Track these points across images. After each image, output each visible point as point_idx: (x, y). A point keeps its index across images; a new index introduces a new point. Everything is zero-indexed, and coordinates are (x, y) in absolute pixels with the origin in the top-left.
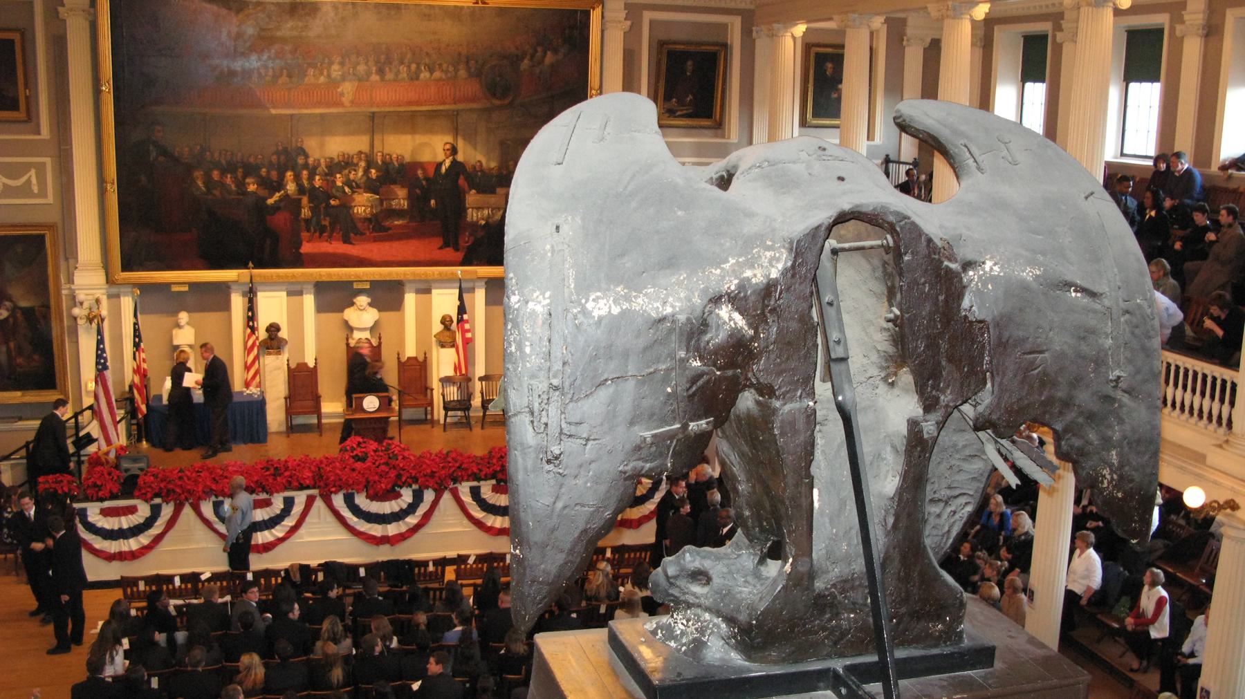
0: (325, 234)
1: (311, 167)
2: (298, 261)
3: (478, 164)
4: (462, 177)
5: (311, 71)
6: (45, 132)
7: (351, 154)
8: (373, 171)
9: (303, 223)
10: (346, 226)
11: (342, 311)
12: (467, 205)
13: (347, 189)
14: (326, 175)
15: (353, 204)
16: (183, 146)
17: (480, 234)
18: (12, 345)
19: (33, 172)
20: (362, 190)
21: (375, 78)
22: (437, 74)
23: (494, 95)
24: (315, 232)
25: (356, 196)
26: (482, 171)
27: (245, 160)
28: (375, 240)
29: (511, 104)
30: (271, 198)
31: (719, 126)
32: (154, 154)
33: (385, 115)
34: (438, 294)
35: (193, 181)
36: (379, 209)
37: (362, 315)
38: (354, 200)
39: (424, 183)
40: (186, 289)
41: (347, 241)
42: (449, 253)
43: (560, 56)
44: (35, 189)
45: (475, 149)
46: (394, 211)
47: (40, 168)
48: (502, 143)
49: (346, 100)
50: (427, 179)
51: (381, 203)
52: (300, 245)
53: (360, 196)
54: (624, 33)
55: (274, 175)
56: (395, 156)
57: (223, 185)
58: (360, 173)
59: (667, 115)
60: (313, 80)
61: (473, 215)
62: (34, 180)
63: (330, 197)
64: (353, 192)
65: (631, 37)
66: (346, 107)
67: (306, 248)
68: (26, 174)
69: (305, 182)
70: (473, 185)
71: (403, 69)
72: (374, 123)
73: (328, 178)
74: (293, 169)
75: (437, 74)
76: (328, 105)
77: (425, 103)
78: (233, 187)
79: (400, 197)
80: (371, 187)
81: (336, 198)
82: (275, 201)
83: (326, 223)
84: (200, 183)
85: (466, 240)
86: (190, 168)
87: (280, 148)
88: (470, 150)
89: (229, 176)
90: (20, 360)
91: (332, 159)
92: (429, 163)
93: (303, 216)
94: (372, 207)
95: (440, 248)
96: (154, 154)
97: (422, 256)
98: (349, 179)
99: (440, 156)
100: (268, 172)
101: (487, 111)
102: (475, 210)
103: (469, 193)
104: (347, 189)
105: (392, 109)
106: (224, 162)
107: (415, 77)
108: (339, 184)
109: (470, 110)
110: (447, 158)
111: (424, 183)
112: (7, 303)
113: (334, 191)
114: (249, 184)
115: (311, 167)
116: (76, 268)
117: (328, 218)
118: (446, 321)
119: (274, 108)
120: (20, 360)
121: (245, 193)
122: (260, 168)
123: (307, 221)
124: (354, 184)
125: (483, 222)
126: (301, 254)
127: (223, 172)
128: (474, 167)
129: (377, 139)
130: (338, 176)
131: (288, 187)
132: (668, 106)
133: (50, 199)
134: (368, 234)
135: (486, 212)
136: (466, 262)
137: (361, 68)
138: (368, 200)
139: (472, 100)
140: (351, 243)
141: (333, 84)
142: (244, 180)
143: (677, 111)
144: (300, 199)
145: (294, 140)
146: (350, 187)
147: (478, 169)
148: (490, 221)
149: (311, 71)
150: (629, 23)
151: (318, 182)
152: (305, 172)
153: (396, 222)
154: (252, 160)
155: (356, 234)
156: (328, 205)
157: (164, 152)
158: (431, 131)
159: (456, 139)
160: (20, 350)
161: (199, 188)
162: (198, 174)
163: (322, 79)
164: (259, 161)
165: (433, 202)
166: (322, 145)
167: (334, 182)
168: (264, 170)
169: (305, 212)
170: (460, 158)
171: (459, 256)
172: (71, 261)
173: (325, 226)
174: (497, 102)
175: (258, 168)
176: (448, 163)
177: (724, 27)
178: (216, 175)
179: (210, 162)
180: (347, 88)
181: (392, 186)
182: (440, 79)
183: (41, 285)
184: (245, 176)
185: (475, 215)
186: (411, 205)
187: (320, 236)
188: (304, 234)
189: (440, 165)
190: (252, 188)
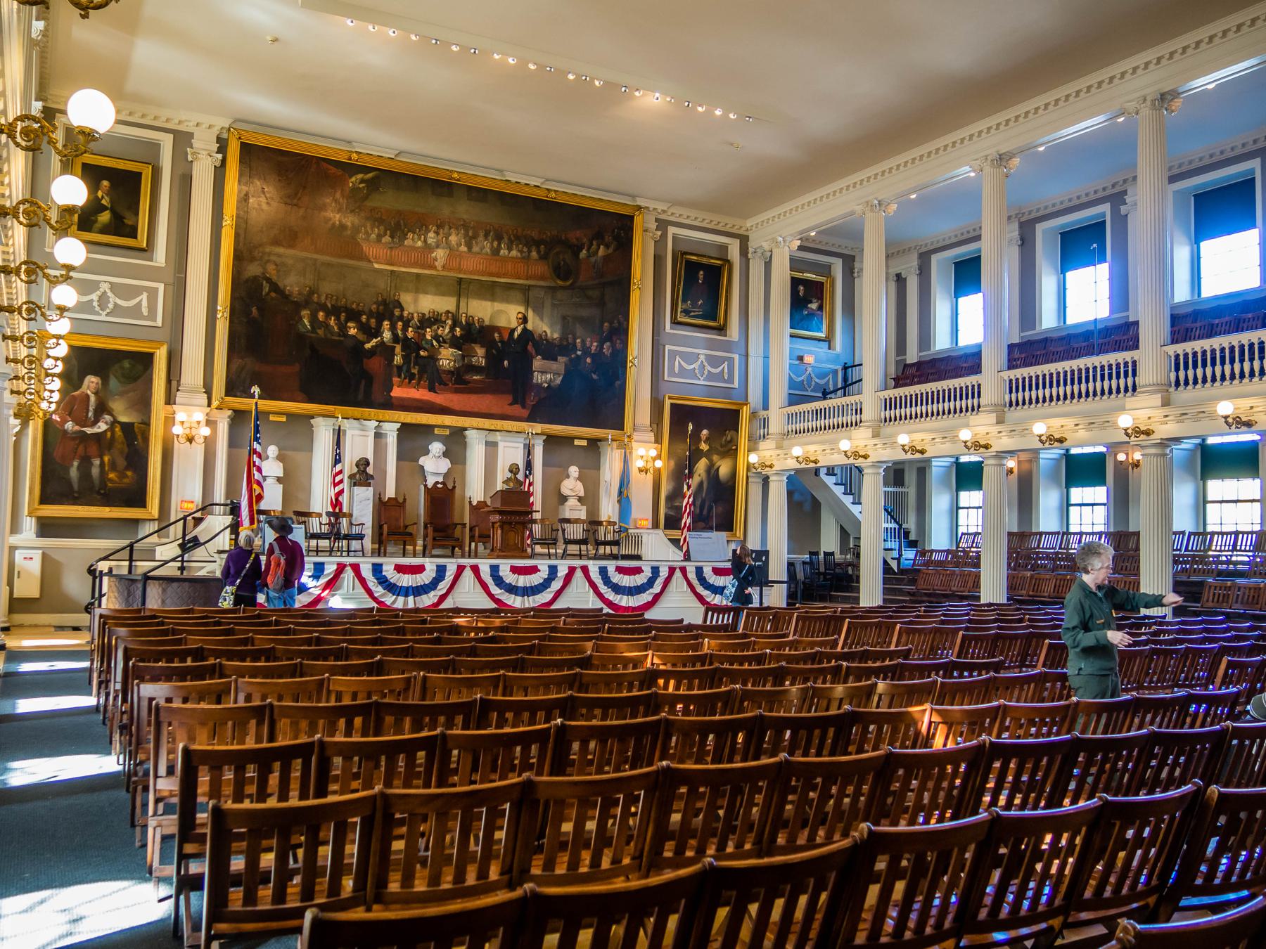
2: (390, 405)
5: (410, 235)
6: (160, 255)
8: (458, 329)
9: (395, 369)
10: (433, 377)
13: (435, 343)
14: (418, 328)
17: (543, 395)
18: (106, 459)
19: (144, 296)
21: (464, 248)
22: (514, 253)
23: (559, 277)
25: (442, 350)
27: (349, 306)
28: (457, 391)
29: (571, 287)
31: (722, 330)
33: (470, 281)
35: (301, 318)
42: (517, 409)
43: (610, 251)
44: (145, 313)
45: (542, 319)
46: (474, 366)
47: (153, 293)
48: (564, 318)
49: (439, 264)
50: (501, 341)
51: (463, 360)
55: (373, 321)
57: (327, 326)
58: (447, 330)
61: (538, 378)
62: (145, 303)
63: (421, 348)
64: (440, 346)
65: (660, 243)
67: (397, 392)
69: (400, 333)
71: (487, 245)
72: (461, 288)
74: (390, 320)
75: (514, 253)
76: (423, 267)
77: (505, 276)
79: (479, 355)
80: (455, 343)
81: (425, 349)
83: (415, 371)
84: (306, 321)
86: (298, 306)
87: (380, 299)
90: (112, 475)
91: (424, 314)
92: (505, 328)
94: (455, 361)
95: (511, 404)
96: (267, 289)
99: (514, 324)
100: (368, 319)
101: (553, 290)
104: (435, 343)
105: (476, 277)
106: (329, 305)
107: (496, 252)
108: (428, 337)
109: (540, 287)
112: (108, 418)
116: (178, 390)
118: (514, 469)
119: (377, 263)
120: (112, 475)
121: (346, 335)
123: (399, 368)
127: (328, 315)
128: (540, 335)
133: (159, 322)
135: (549, 376)
136: (531, 419)
137: (453, 239)
139: (542, 278)
141: (428, 248)
142: (346, 323)
145: (392, 293)
146: (438, 341)
149: (410, 235)
150: (659, 233)
151: (410, 334)
152: (400, 323)
154: (354, 306)
157: (275, 287)
158: (508, 301)
160: (113, 467)
162: (305, 313)
164: (360, 308)
165: (506, 362)
166: (416, 301)
167: (424, 335)
169: (398, 360)
170: (530, 326)
171: (525, 413)
173: (414, 374)
174: (560, 283)
175: (360, 313)
176: (520, 329)
177: (724, 248)
178: (321, 315)
179: (317, 303)
180: (440, 254)
182: (517, 258)
183: (144, 404)
184: (347, 320)
187: (410, 382)
188: (396, 380)
189: (513, 330)
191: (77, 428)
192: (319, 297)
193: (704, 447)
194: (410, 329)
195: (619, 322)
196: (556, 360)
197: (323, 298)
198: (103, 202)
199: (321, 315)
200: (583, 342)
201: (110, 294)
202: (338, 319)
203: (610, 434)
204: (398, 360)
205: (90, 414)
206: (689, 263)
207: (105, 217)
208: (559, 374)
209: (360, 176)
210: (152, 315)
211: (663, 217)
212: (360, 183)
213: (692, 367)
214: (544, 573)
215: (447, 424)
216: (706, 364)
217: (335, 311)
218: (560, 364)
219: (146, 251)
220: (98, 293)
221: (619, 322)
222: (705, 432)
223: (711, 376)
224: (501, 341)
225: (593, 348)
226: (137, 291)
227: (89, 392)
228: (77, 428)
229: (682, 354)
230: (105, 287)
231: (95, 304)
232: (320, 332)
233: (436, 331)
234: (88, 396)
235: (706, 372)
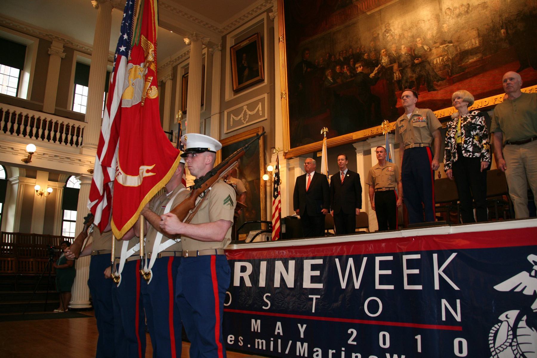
15: (432, 58)
19: (260, 105)
57: (342, 73)
62: (260, 109)
68: (257, 107)
78: (348, 74)
82: (375, 74)
84: (329, 78)
89: (345, 67)
93: (395, 79)
96: (305, 68)
106: (342, 59)
114: (357, 68)
122: (364, 54)
126: (397, 109)
127: (342, 65)
131: (383, 61)
134: (448, 77)
140: (435, 90)
142: (355, 66)
144: (392, 67)
153: (471, 61)
154: (358, 51)
162: (328, 72)
168: (366, 55)
169: (397, 75)
190: (360, 70)
198: (245, 65)
201: (247, 111)
202: (348, 65)
207: (246, 72)
210: (263, 115)
217: (346, 61)
220: (243, 112)
226: (256, 103)
227: (236, 168)
230: (245, 107)
232: (339, 81)
234: (236, 170)
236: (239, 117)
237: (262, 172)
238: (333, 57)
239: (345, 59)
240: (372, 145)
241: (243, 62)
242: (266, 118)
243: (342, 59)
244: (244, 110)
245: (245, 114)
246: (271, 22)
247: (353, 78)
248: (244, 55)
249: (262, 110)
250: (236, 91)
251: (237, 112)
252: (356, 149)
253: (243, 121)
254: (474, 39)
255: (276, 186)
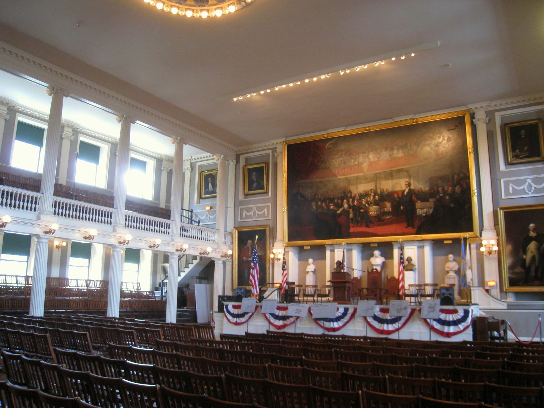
0: (359, 224)
1: (353, 197)
3: (420, 189)
4: (413, 195)
7: (368, 190)
8: (377, 197)
9: (350, 220)
11: (369, 259)
12: (417, 208)
13: (367, 205)
14: (359, 200)
15: (369, 211)
16: (308, 193)
19: (266, 209)
20: (372, 205)
24: (355, 223)
26: (422, 192)
28: (379, 225)
30: (339, 210)
32: (299, 198)
34: (407, 249)
36: (380, 212)
37: (377, 260)
38: (369, 209)
39: (398, 199)
40: (309, 248)
41: (367, 226)
42: (410, 229)
49: (365, 170)
50: (399, 198)
52: (349, 228)
53: (372, 207)
54: (487, 124)
55: (340, 201)
56: (385, 189)
57: (321, 206)
58: (372, 198)
59: (515, 158)
60: (353, 164)
61: (419, 212)
62: (266, 212)
63: (361, 208)
64: (369, 206)
66: (365, 172)
67: (352, 230)
69: (351, 204)
70: (418, 199)
73: (359, 201)
78: (325, 208)
79: (388, 206)
80: (376, 203)
81: (363, 209)
83: (359, 219)
85: (417, 223)
88: (416, 184)
89: (324, 203)
91: (361, 193)
92: (399, 191)
93: (350, 217)
94: (377, 212)
95: (406, 227)
97: (398, 231)
98: (367, 201)
99: (404, 187)
100: (337, 201)
102: (420, 210)
103: (417, 202)
104: (367, 205)
106: (322, 198)
108: (364, 203)
110: (407, 188)
111: (398, 199)
113: (362, 206)
114: (331, 206)
115: (353, 197)
117: (360, 217)
119: (339, 176)
123: (352, 219)
124: (369, 203)
125: (424, 215)
127: (322, 202)
128: (419, 191)
129: (378, 183)
130: (363, 200)
131: (345, 206)
132: (515, 154)
133: (270, 218)
135: (425, 210)
136: (418, 233)
138: (375, 209)
140: (369, 227)
143: (520, 155)
144: (349, 210)
146: (368, 204)
147: (420, 191)
148: (428, 214)
150: (488, 119)
151: (356, 203)
152: (351, 199)
153: (387, 217)
154: (332, 196)
155: (371, 223)
156: (360, 212)
157: (302, 196)
159: (410, 179)
161: (314, 209)
162: (313, 204)
163: (356, 163)
164: (334, 197)
166: (357, 188)
167: (362, 202)
169: (351, 215)
170: (412, 187)
171: (414, 230)
172: (275, 239)
175: (334, 199)
176: (407, 190)
178: (319, 203)
180: (365, 165)
181: (385, 202)
184: (329, 203)
185: (420, 212)
186: (392, 209)
187: (357, 225)
188: (351, 225)
189: (404, 191)
190: (332, 207)
191: (246, 259)
192: (318, 196)
193: (532, 234)
194: (355, 201)
195: (463, 173)
196: (428, 201)
197: (320, 196)
198: (254, 180)
199: (319, 203)
200: (443, 189)
201: (256, 211)
202: (326, 203)
203: (467, 235)
204: (351, 215)
205: (250, 254)
206: (511, 128)
207: (255, 185)
208: (431, 208)
209: (330, 142)
211: (491, 109)
212: (330, 145)
213: (521, 188)
214: (461, 314)
215: (374, 241)
216: (532, 184)
217: (324, 200)
218: (431, 203)
219: (267, 192)
221: (463, 173)
222: (532, 225)
223: (537, 190)
224: (399, 198)
225: (449, 191)
228: (246, 259)
229: (514, 182)
230: (255, 208)
231: (252, 215)
233: (367, 199)
234: (249, 247)
235: (533, 188)
236: (250, 213)
237: (268, 252)
238: (317, 196)
239: (324, 198)
240: (335, 247)
241: (253, 177)
242: (270, 218)
243: (322, 198)
244: (254, 210)
245: (255, 212)
246: (275, 159)
247: (328, 211)
248: (254, 173)
249: (267, 213)
250: (246, 195)
251: (248, 210)
252: (326, 248)
253: (253, 217)
254: (390, 207)
255: (284, 265)
